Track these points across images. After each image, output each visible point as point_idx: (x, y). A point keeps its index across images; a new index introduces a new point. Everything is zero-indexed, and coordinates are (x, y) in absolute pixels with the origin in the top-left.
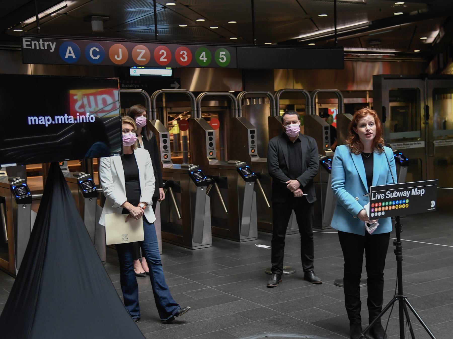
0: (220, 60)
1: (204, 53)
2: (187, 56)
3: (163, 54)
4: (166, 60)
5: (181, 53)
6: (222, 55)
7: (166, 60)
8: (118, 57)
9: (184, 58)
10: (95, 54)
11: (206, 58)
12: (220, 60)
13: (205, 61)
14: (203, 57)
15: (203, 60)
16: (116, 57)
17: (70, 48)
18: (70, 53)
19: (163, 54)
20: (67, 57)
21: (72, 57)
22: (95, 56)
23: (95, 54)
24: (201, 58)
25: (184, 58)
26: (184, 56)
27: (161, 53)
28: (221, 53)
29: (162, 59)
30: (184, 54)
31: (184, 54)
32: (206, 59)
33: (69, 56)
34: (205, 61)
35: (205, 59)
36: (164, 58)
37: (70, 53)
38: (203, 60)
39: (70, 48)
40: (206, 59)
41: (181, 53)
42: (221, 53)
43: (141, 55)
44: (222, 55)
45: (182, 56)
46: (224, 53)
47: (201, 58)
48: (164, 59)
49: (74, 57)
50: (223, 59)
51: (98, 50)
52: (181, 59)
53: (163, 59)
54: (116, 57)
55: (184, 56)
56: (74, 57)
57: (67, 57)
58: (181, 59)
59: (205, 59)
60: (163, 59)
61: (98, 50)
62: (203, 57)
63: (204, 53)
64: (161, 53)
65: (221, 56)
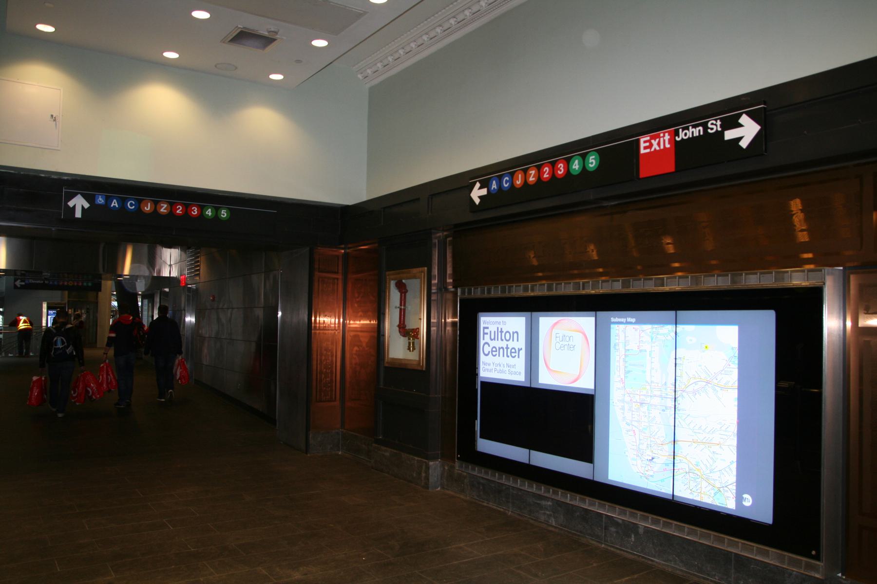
0: (222, 215)
1: (210, 210)
4: (181, 212)
5: (193, 208)
7: (181, 212)
8: (147, 208)
9: (194, 212)
10: (131, 205)
12: (222, 215)
13: (210, 215)
16: (146, 208)
17: (115, 201)
18: (115, 203)
19: (179, 208)
20: (112, 206)
21: (115, 206)
22: (131, 206)
23: (131, 205)
24: (207, 213)
25: (194, 212)
27: (178, 207)
28: (223, 211)
29: (178, 212)
30: (195, 209)
33: (114, 206)
34: (210, 215)
35: (210, 214)
36: (180, 211)
37: (115, 203)
39: (115, 201)
41: (193, 208)
42: (223, 211)
43: (164, 208)
45: (193, 210)
46: (225, 211)
47: (207, 213)
48: (180, 211)
49: (117, 206)
50: (224, 215)
51: (134, 203)
52: (192, 212)
54: (146, 208)
56: (117, 206)
57: (112, 206)
58: (192, 212)
59: (210, 214)
61: (134, 203)
62: (209, 212)
63: (210, 210)
64: (178, 207)
65: (222, 213)
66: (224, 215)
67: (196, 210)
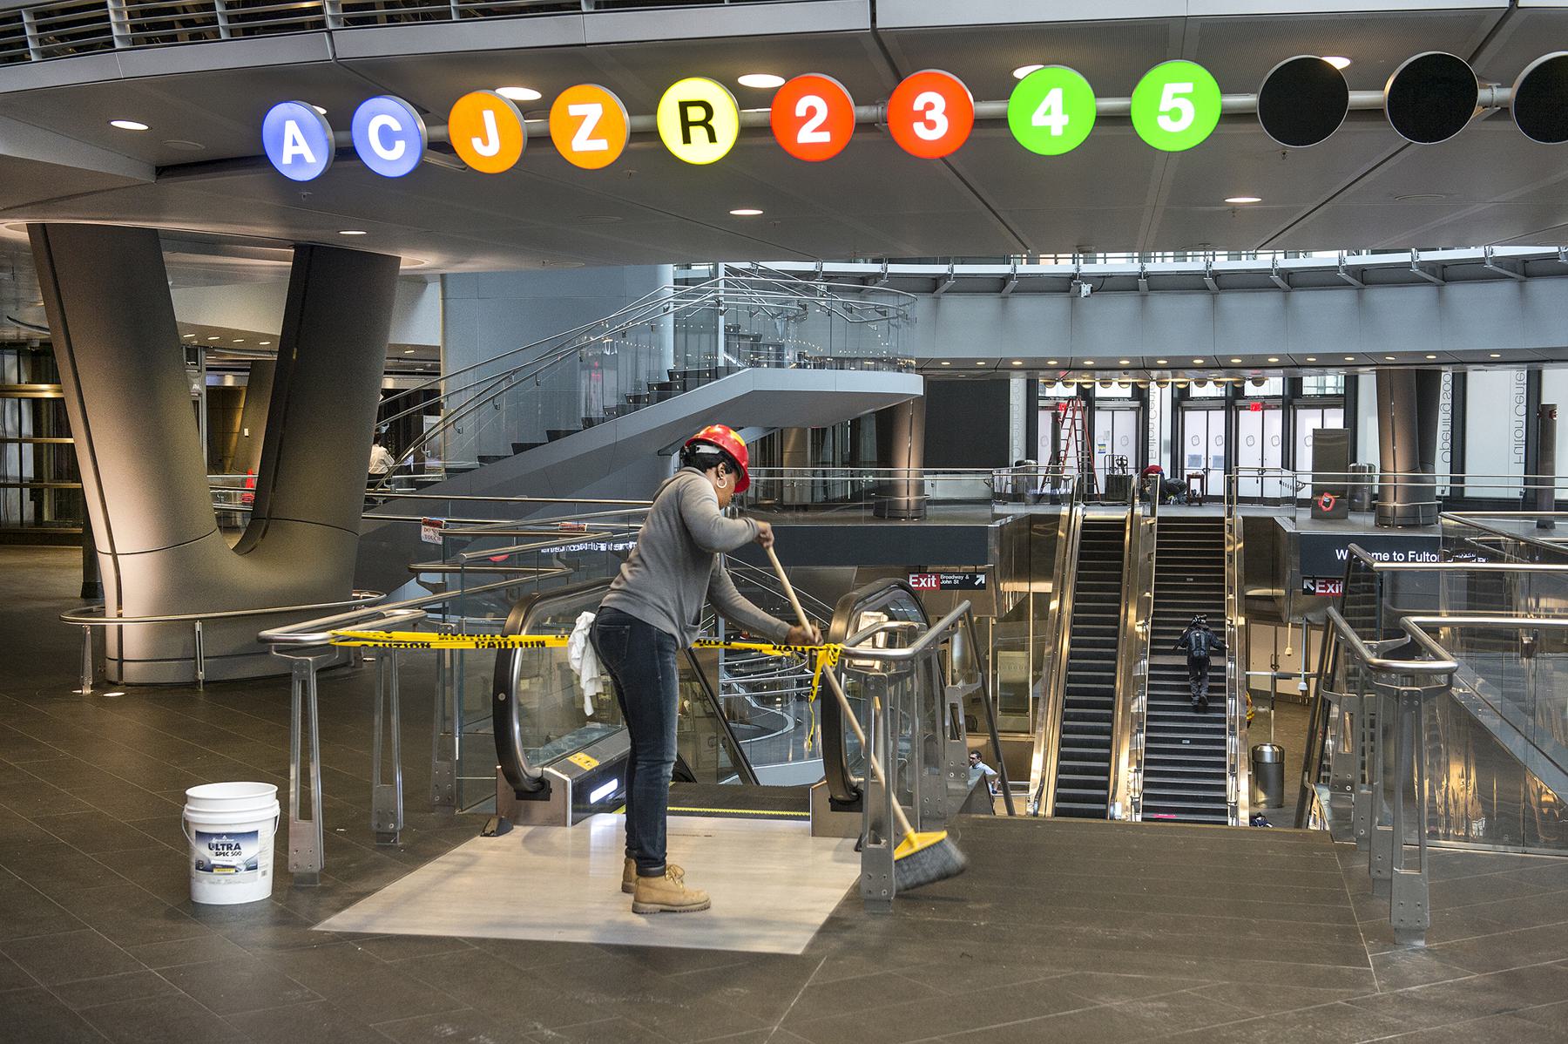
1: (1055, 97)
2: (946, 113)
3: (811, 112)
6: (1176, 96)
9: (931, 125)
11: (1064, 113)
13: (1057, 131)
14: (1048, 113)
15: (1049, 128)
19: (811, 112)
25: (931, 125)
26: (929, 115)
28: (1170, 89)
30: (929, 106)
31: (929, 106)
32: (1065, 120)
34: (1057, 131)
36: (819, 129)
38: (1049, 128)
40: (1065, 120)
41: (918, 105)
42: (1170, 89)
44: (1176, 96)
45: (920, 116)
46: (1187, 88)
48: (819, 129)
50: (1175, 114)
53: (816, 130)
55: (929, 115)
58: (919, 129)
60: (816, 130)
62: (1048, 113)
63: (1055, 97)
64: (801, 110)
65: (1166, 104)
66: (1175, 114)
67: (938, 115)
